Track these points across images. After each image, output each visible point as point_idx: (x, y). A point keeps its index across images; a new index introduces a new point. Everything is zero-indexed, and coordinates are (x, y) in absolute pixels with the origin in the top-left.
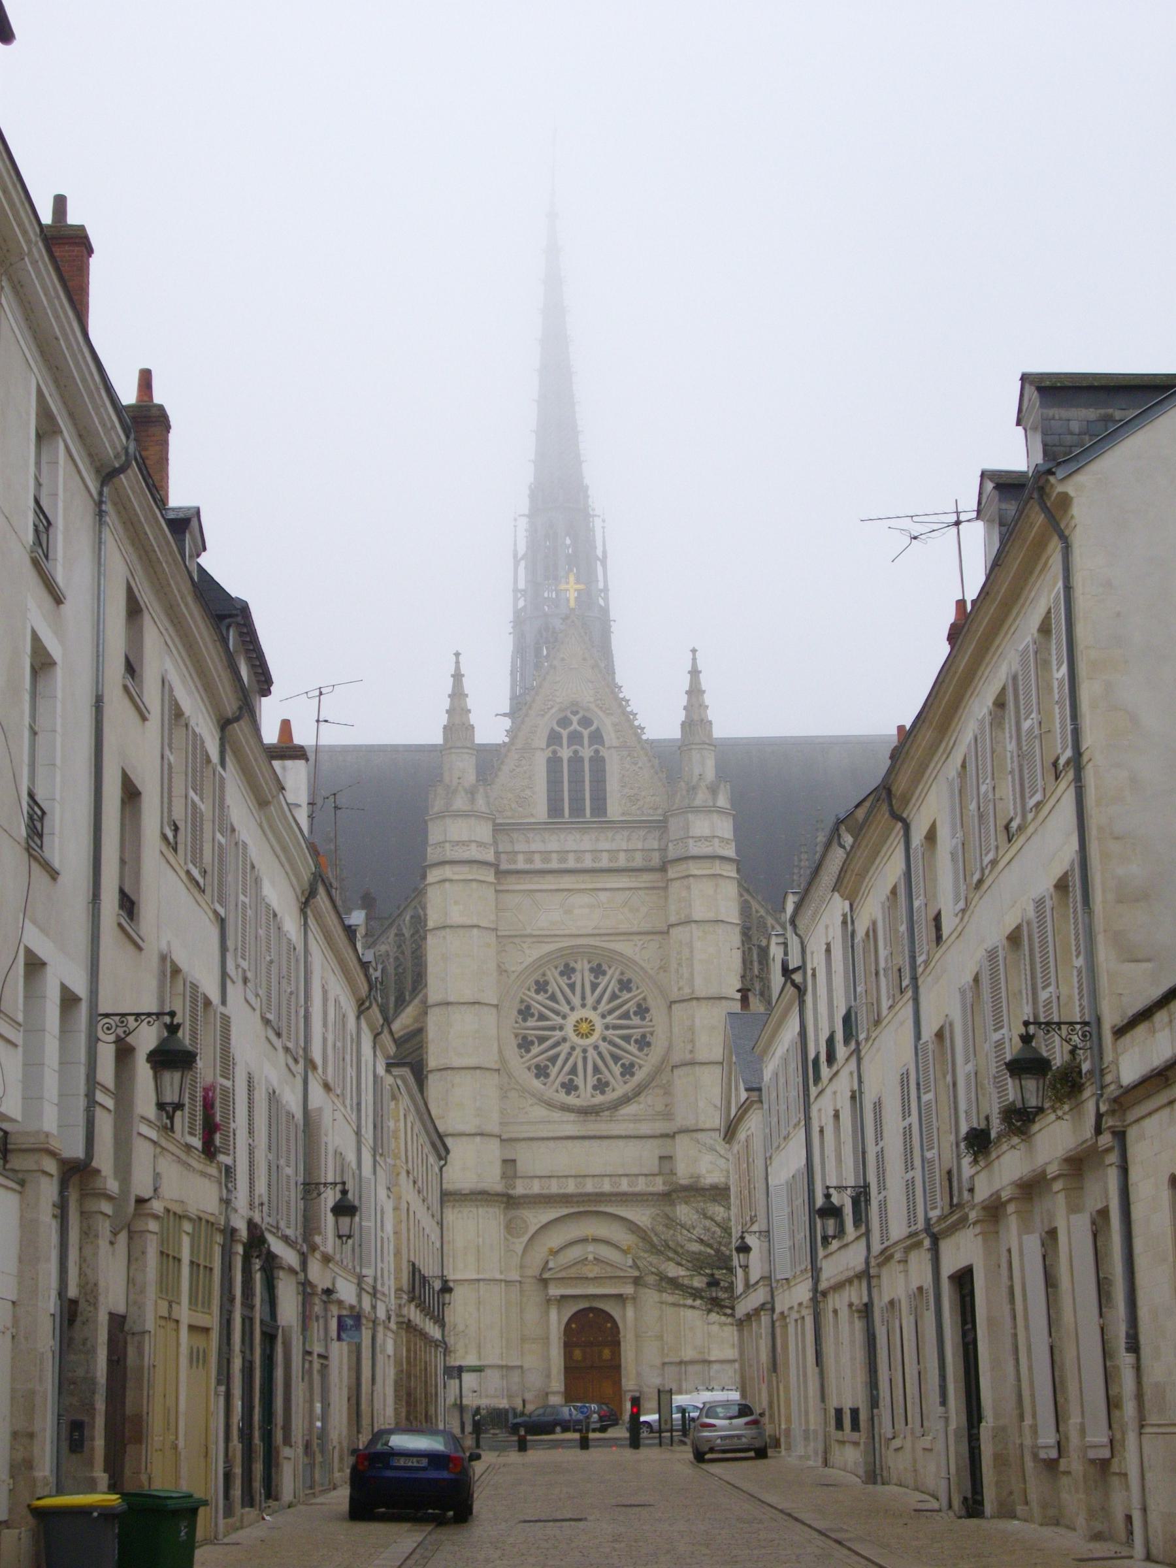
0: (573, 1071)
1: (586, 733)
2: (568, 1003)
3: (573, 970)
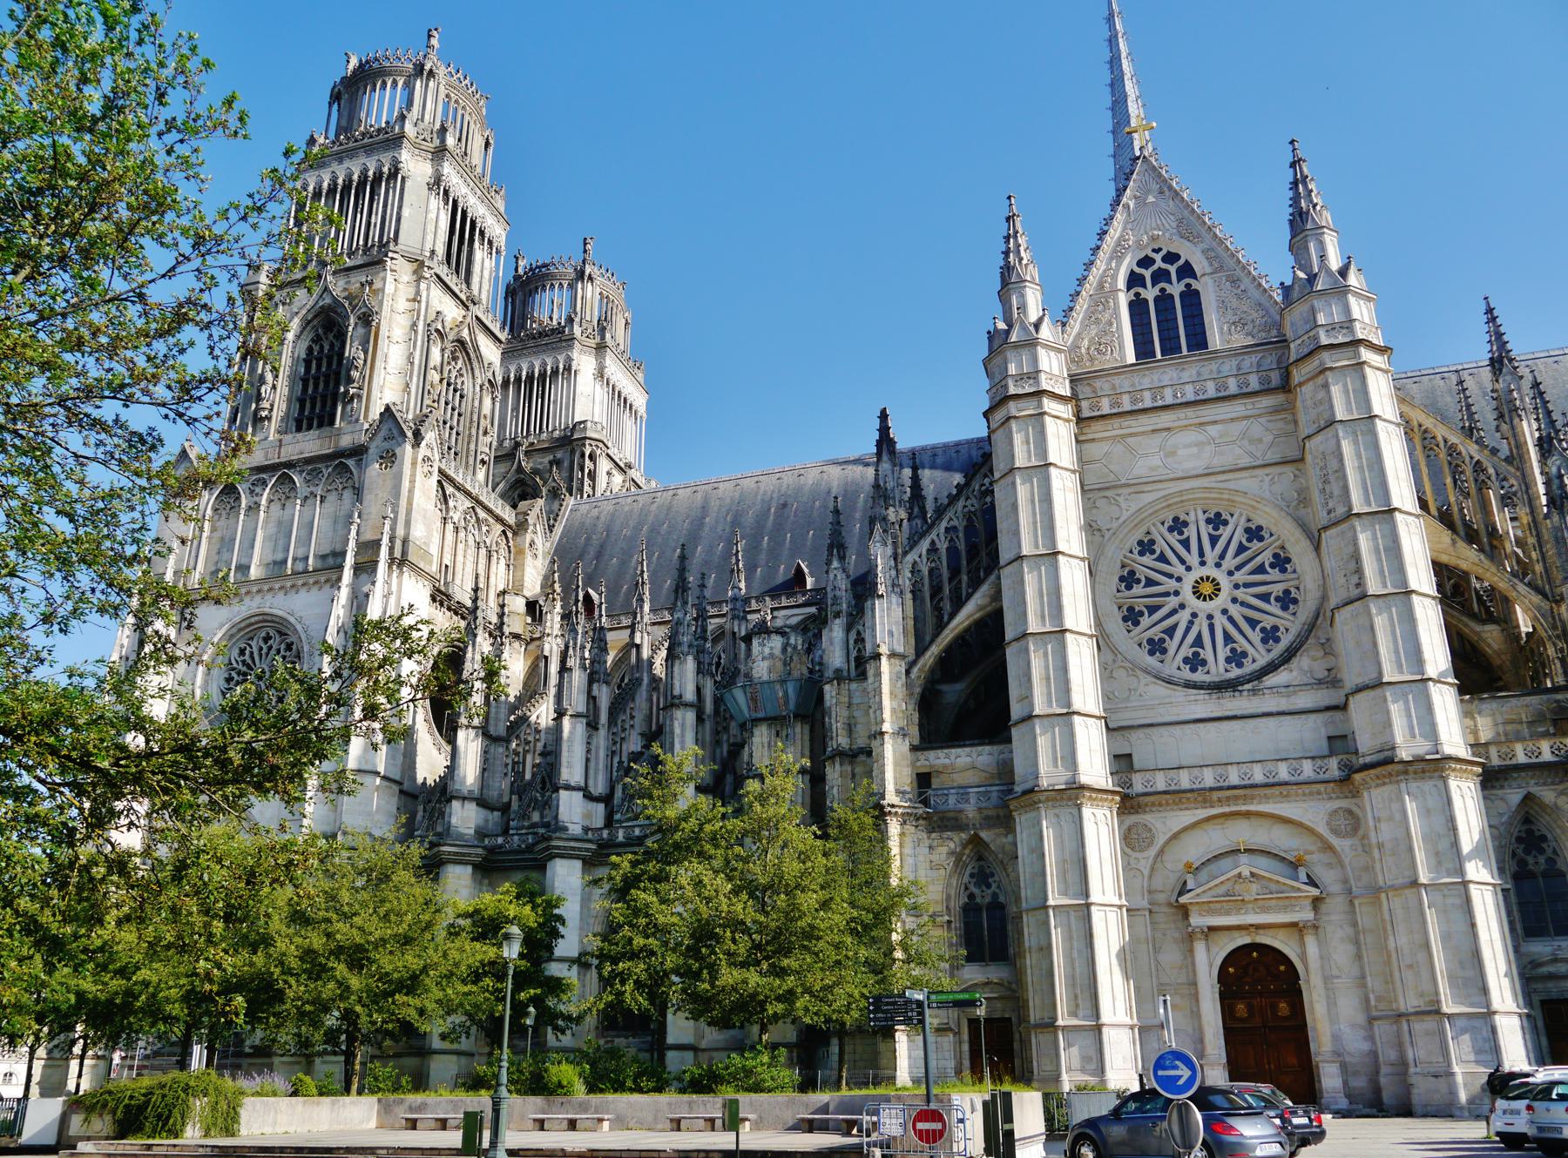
0: (1198, 642)
1: (1173, 269)
2: (1183, 562)
3: (1186, 524)
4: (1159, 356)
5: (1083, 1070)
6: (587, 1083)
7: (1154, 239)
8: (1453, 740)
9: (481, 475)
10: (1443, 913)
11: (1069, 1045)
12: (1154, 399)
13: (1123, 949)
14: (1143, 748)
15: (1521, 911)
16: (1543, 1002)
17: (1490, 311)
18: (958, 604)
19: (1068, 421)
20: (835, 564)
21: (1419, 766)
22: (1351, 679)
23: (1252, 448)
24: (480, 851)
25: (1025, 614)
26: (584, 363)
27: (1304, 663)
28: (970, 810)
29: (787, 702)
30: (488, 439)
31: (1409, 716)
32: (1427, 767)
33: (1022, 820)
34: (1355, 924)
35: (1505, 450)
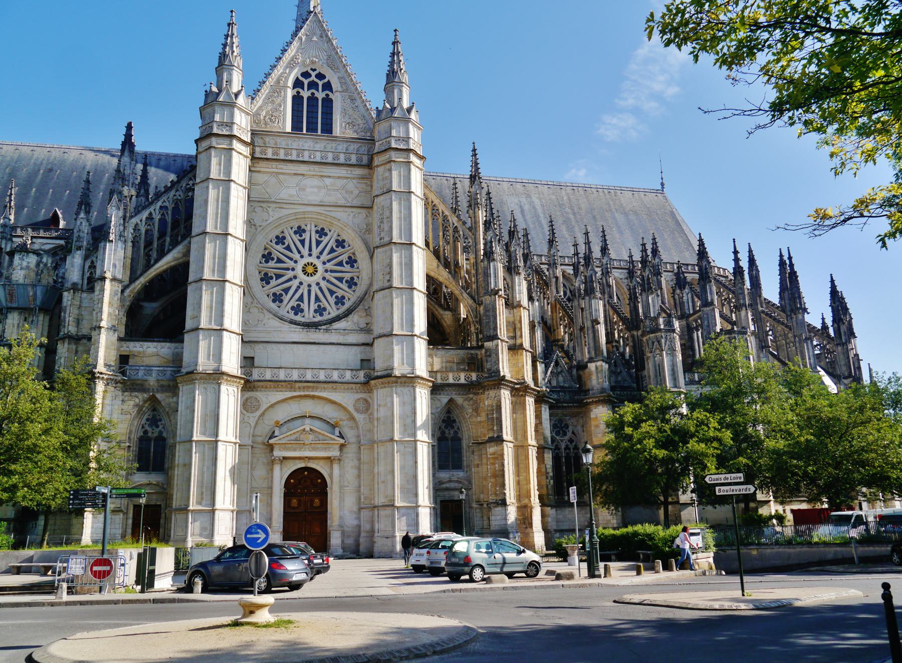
0: (301, 299)
1: (320, 83)
2: (299, 252)
3: (304, 231)
4: (305, 132)
5: (201, 535)
7: (313, 62)
8: (421, 369)
10: (403, 455)
11: (194, 521)
12: (298, 156)
13: (234, 467)
14: (261, 354)
15: (439, 457)
16: (441, 501)
17: (474, 150)
18: (162, 254)
19: (246, 157)
20: (82, 215)
21: (403, 380)
22: (377, 330)
23: (347, 196)
25: (203, 267)
27: (356, 319)
28: (152, 381)
31: (403, 353)
32: (407, 380)
33: (183, 389)
34: (359, 459)
35: (469, 225)
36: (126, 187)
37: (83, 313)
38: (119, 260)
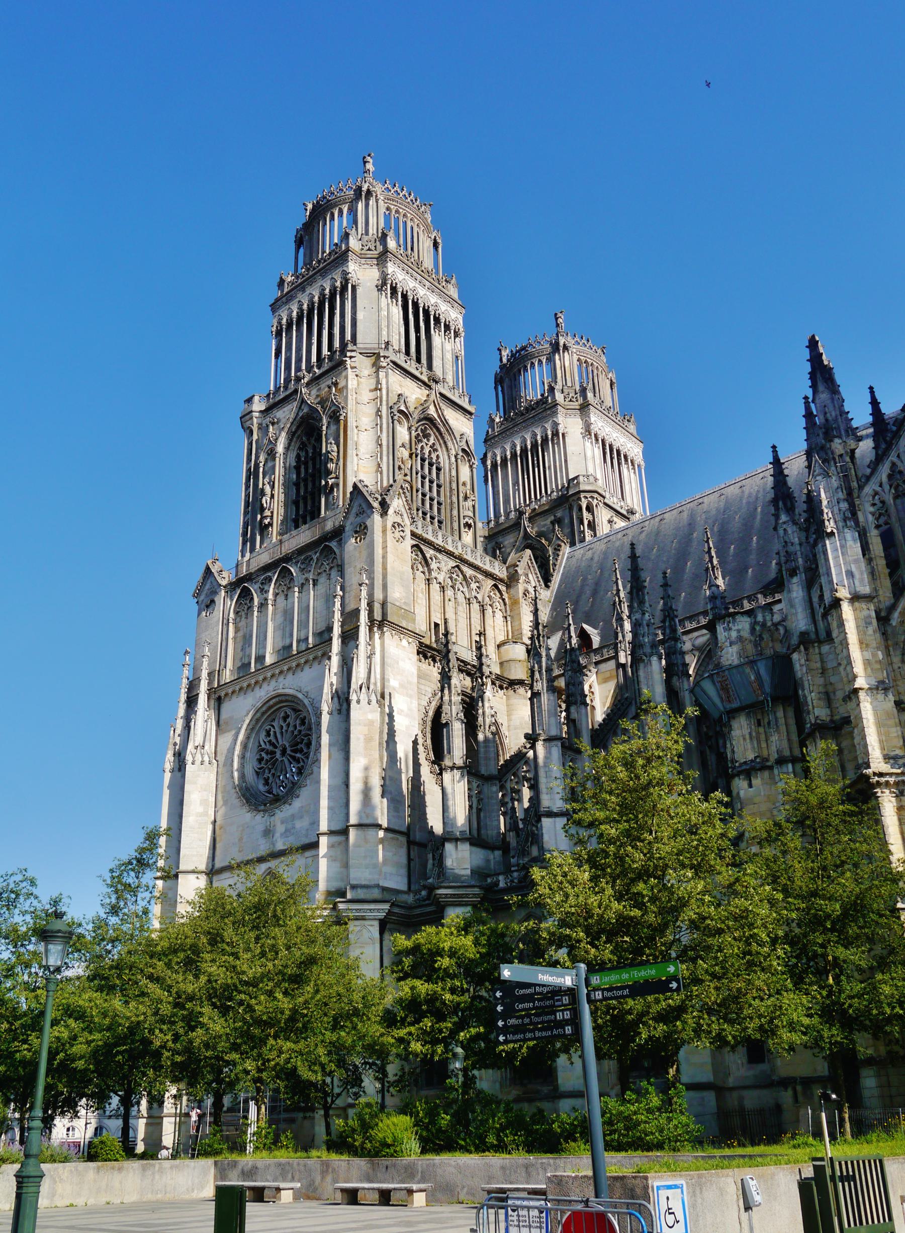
6: (422, 1139)
9: (468, 537)
20: (783, 518)
24: (476, 891)
26: (569, 423)
29: (761, 685)
30: (469, 503)
36: (837, 441)
37: (833, 679)
38: (856, 561)
